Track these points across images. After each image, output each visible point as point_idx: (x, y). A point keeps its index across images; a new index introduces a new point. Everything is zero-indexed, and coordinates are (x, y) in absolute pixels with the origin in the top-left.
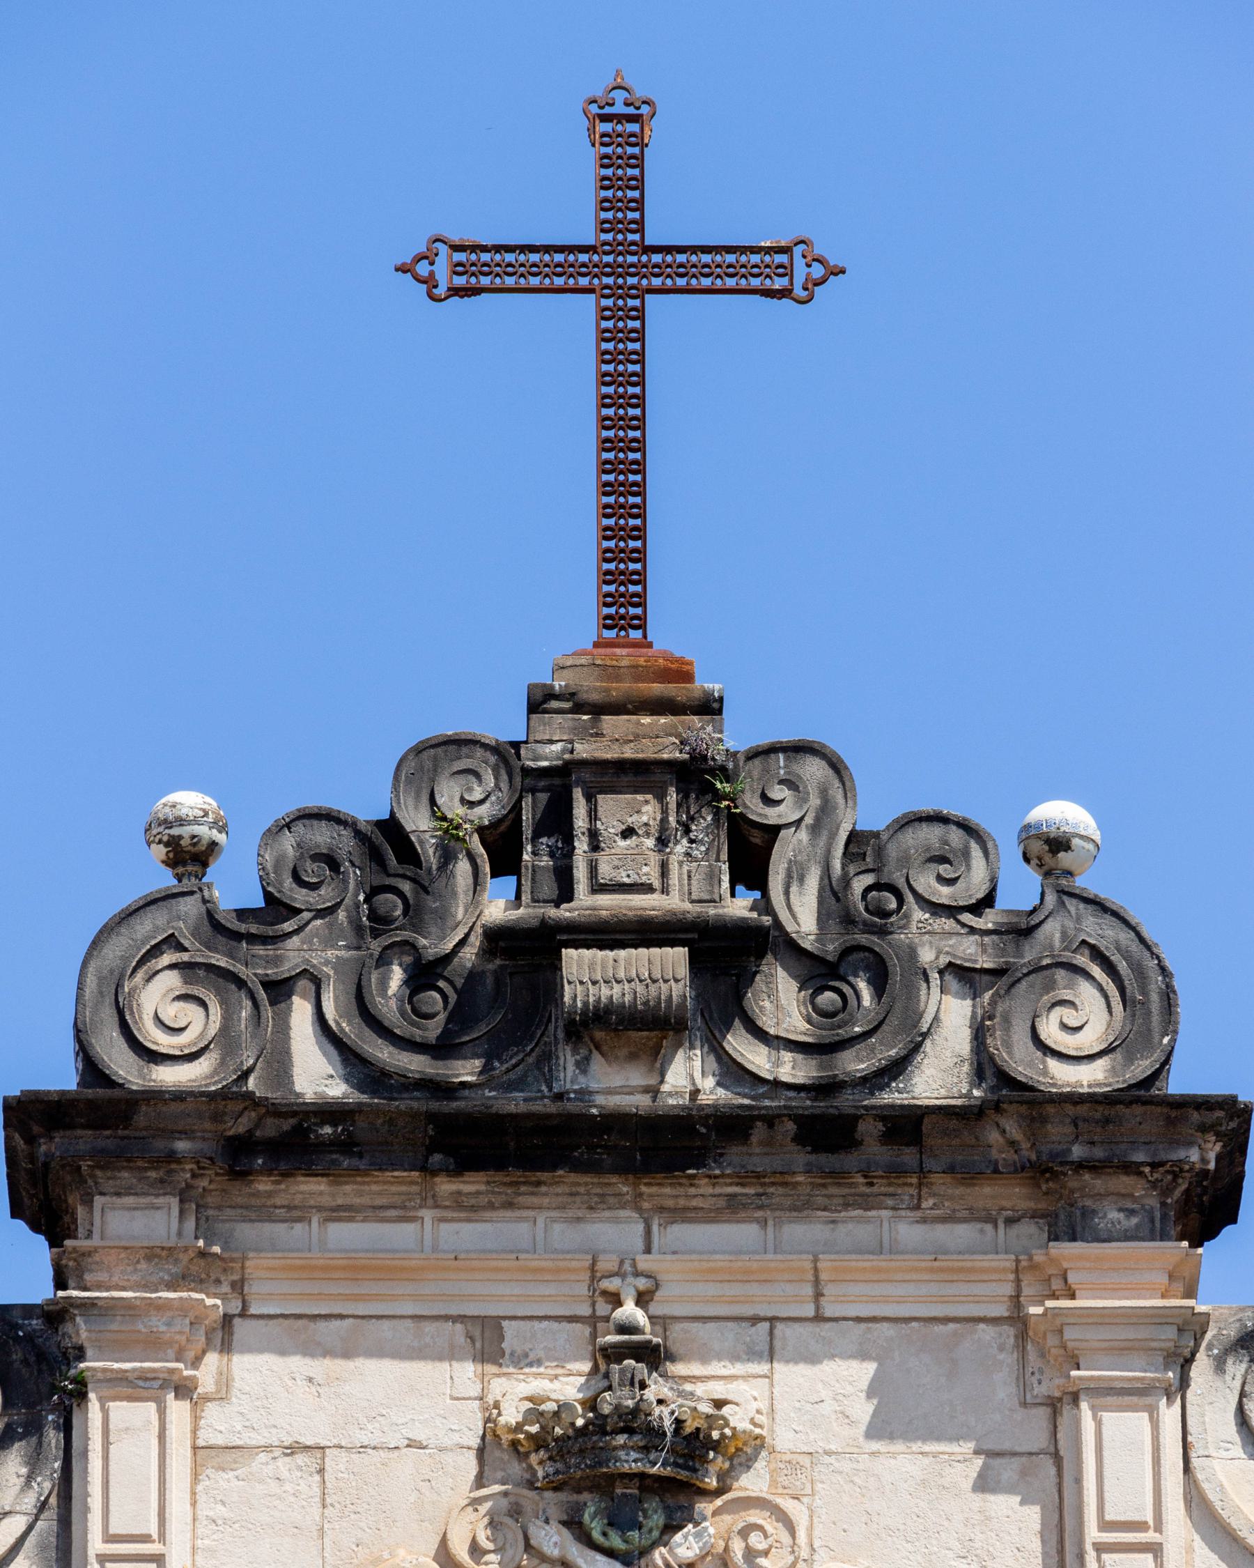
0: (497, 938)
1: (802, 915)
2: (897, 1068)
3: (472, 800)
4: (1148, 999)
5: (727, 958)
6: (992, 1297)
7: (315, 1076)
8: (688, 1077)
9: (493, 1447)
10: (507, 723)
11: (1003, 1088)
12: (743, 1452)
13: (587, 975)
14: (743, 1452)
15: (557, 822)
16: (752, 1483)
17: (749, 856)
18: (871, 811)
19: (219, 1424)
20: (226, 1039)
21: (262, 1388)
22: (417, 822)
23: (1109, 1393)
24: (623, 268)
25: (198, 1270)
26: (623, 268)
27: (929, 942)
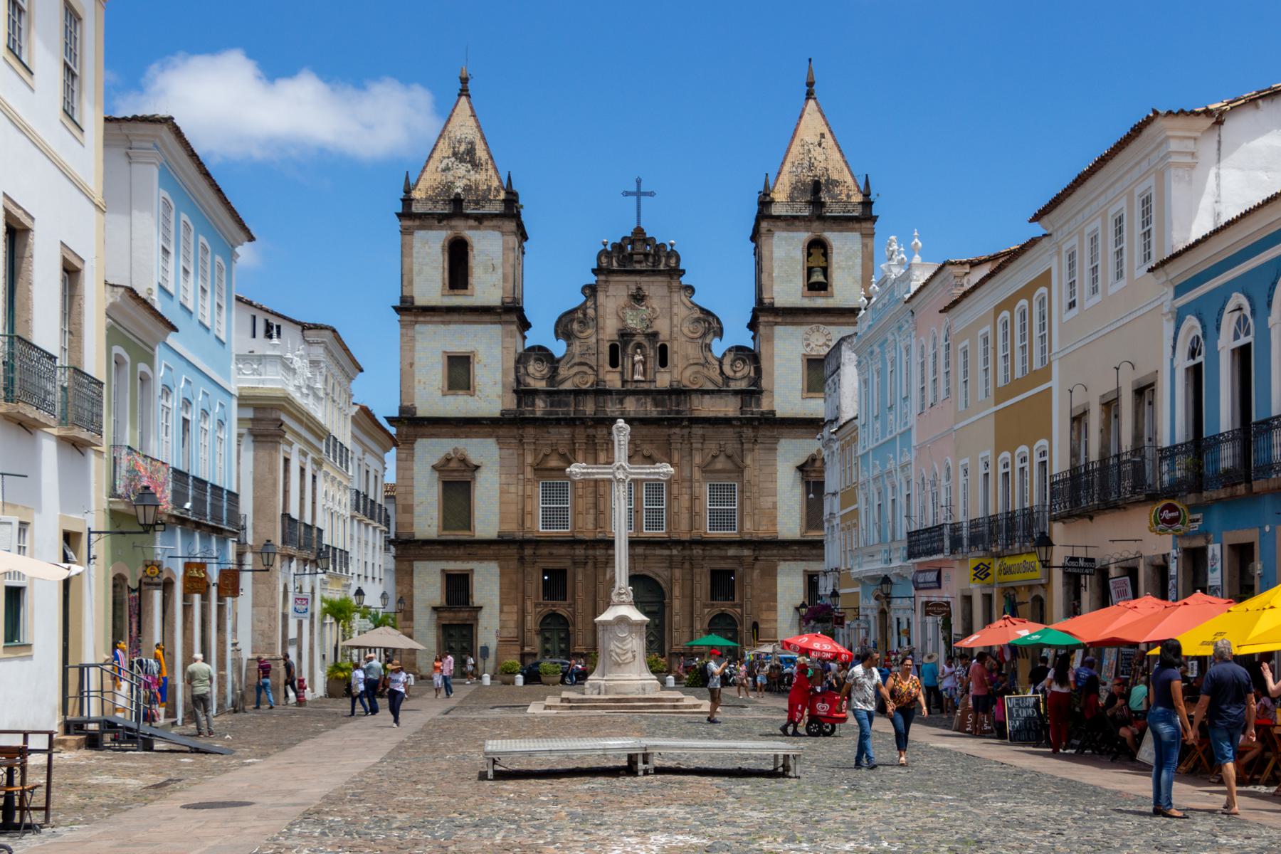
4: (678, 259)
5: (646, 255)
13: (636, 257)
26: (639, 194)
27: (661, 254)
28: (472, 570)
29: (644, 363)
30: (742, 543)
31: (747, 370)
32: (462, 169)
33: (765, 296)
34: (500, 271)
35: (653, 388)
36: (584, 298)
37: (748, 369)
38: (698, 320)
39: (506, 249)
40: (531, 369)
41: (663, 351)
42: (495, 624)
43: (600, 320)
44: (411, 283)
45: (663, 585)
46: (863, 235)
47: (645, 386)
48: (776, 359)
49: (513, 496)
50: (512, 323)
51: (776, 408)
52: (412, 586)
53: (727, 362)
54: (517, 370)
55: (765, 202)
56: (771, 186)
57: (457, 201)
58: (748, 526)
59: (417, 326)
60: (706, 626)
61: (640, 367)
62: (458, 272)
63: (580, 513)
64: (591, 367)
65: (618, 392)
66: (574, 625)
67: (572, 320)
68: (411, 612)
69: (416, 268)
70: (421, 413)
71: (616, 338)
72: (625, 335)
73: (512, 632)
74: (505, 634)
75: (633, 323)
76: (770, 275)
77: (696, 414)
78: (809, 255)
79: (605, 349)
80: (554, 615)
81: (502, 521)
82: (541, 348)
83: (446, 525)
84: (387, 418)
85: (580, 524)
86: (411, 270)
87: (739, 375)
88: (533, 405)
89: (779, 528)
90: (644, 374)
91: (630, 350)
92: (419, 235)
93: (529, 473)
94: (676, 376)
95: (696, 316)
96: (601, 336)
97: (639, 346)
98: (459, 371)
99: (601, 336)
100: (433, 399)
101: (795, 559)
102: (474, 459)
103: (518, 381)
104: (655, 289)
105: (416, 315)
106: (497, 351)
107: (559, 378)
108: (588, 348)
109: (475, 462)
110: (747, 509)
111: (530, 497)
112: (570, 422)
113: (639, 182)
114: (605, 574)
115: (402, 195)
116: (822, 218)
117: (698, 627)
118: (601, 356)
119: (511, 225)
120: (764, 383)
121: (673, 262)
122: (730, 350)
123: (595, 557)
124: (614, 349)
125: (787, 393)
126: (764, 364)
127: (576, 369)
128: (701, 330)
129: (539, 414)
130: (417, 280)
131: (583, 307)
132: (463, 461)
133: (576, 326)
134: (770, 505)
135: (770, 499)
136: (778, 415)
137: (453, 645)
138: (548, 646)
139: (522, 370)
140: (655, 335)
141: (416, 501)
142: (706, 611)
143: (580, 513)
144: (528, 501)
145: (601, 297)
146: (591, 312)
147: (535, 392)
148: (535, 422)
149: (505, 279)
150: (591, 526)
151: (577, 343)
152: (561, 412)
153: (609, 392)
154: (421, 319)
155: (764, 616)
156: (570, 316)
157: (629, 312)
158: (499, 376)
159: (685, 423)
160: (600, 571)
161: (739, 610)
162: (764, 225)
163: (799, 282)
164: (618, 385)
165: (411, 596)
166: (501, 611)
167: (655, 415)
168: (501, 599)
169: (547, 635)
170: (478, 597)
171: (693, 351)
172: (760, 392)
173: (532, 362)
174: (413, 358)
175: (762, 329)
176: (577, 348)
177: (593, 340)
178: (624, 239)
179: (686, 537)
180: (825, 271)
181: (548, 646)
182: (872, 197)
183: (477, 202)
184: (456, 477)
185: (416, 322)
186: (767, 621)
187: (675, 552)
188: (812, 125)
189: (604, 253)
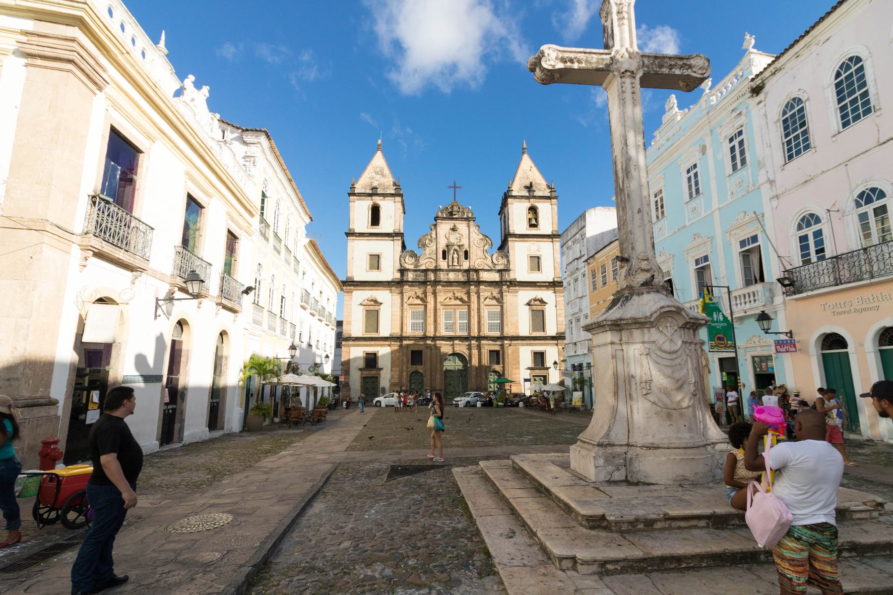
24: (455, 187)
26: (455, 187)
32: (378, 177)
37: (505, 261)
41: (466, 253)
42: (389, 376)
47: (458, 268)
53: (494, 257)
57: (375, 188)
61: (456, 260)
65: (446, 270)
70: (355, 279)
74: (393, 381)
75: (453, 240)
80: (416, 372)
82: (412, 251)
85: (428, 329)
91: (452, 252)
98: (375, 261)
100: (360, 273)
101: (527, 345)
102: (379, 300)
104: (462, 226)
112: (424, 283)
116: (535, 197)
120: (511, 267)
121: (470, 215)
124: (444, 252)
125: (520, 271)
126: (511, 258)
132: (376, 301)
146: (434, 236)
147: (408, 270)
153: (440, 270)
155: (514, 372)
162: (509, 200)
163: (525, 224)
164: (446, 268)
171: (480, 253)
175: (510, 243)
180: (536, 220)
184: (372, 308)
188: (526, 162)
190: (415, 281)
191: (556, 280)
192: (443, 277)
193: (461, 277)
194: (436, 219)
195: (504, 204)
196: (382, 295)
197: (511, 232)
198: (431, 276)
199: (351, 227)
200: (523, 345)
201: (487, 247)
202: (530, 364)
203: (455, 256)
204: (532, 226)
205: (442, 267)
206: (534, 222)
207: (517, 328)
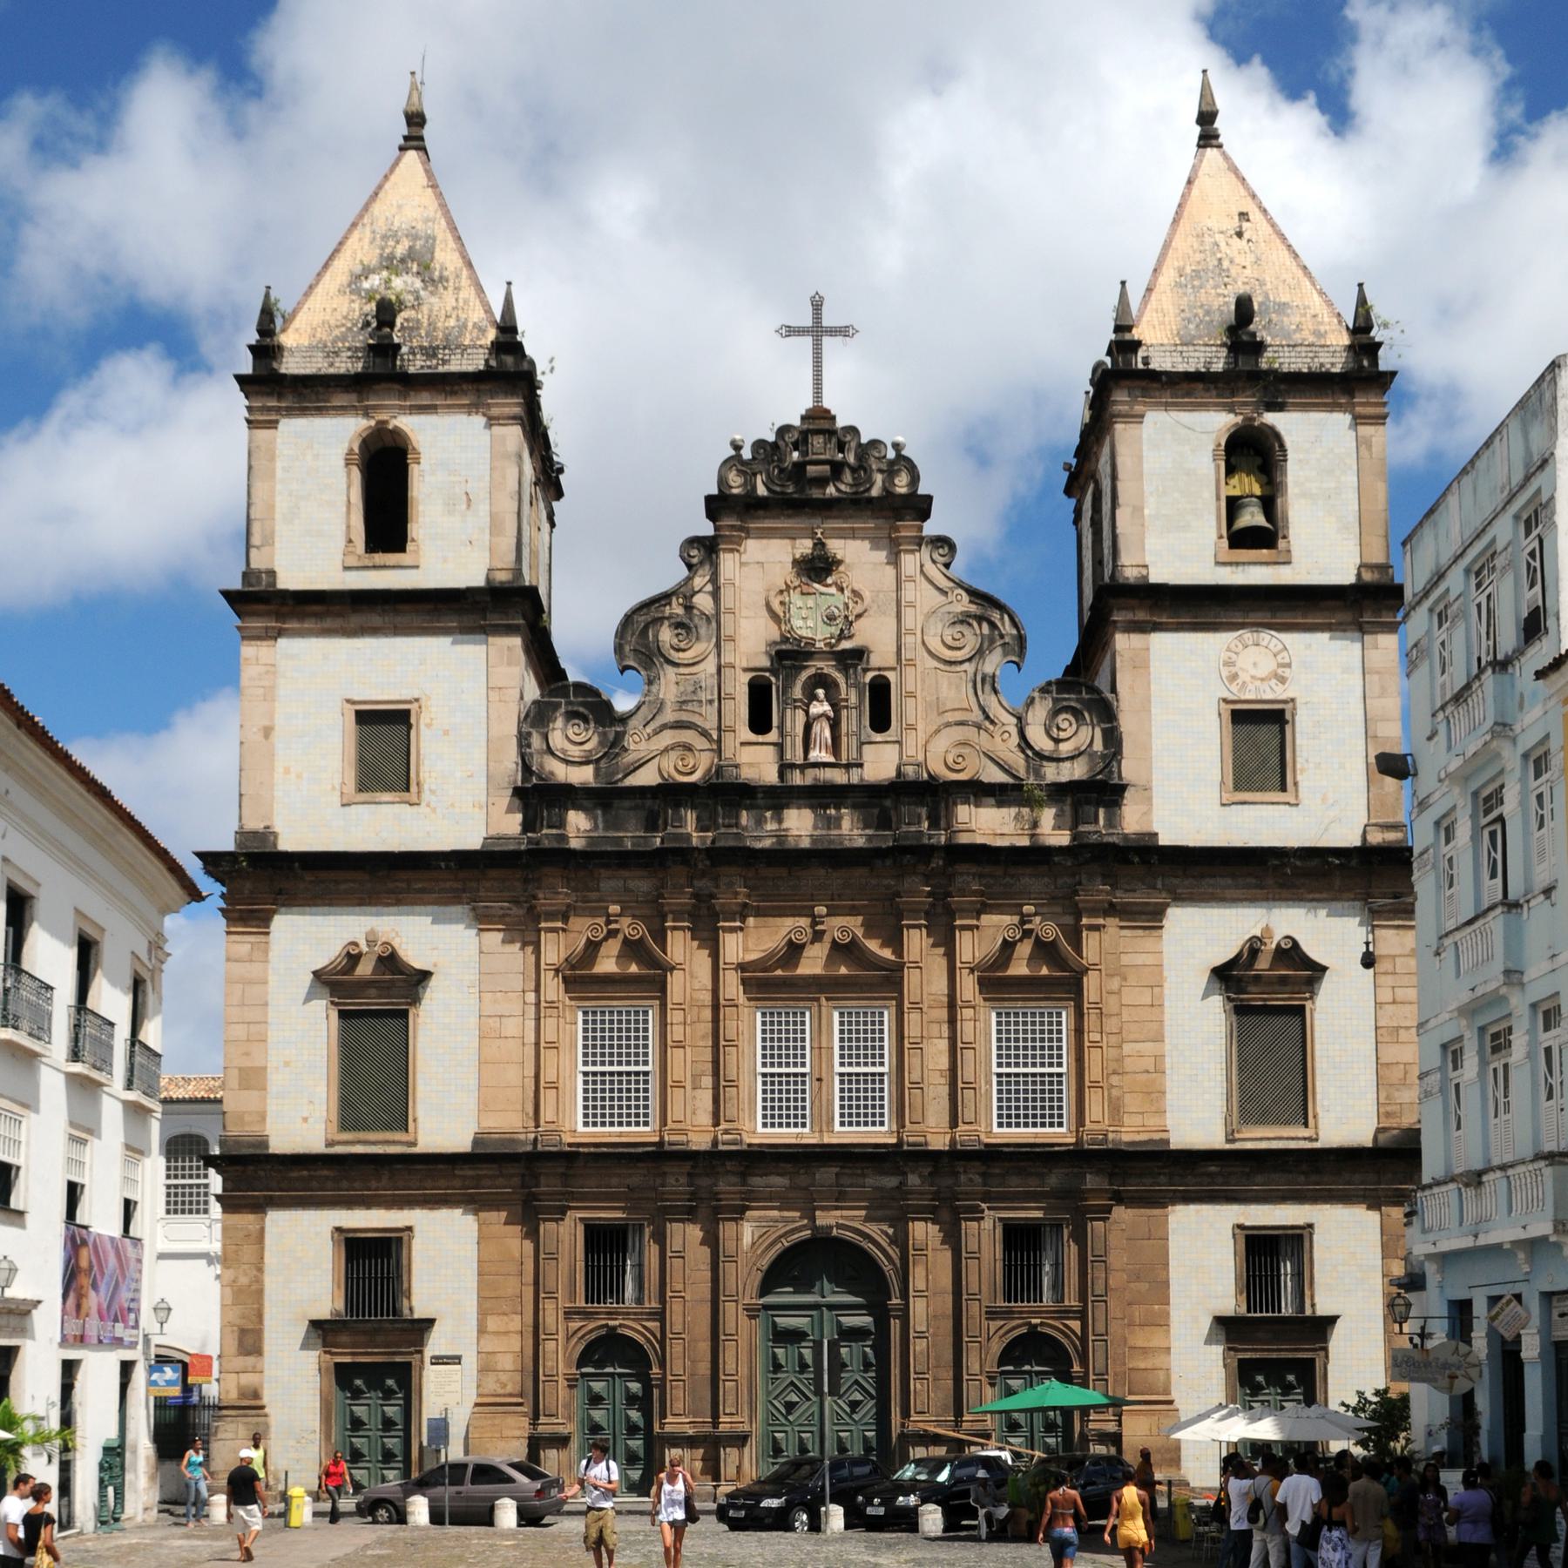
0: (795, 464)
1: (851, 459)
2: (868, 490)
3: (791, 437)
4: (915, 479)
5: (837, 468)
6: (885, 533)
7: (762, 491)
8: (831, 490)
9: (795, 562)
10: (797, 422)
11: (888, 493)
12: (840, 562)
14: (840, 562)
15: (805, 441)
16: (841, 568)
17: (841, 447)
18: (864, 440)
19: (744, 558)
20: (744, 485)
21: (753, 548)
22: (781, 443)
23: (907, 551)
24: (818, 331)
25: (741, 529)
26: (818, 331)
28: (410, 1229)
29: (835, 725)
30: (1079, 1157)
31: (1083, 736)
33: (1125, 559)
34: (483, 509)
35: (855, 780)
36: (685, 572)
38: (964, 620)
39: (496, 455)
40: (557, 739)
43: (726, 619)
44: (269, 540)
45: (887, 1267)
46: (1358, 420)
47: (838, 777)
48: (1155, 710)
49: (513, 1045)
50: (509, 630)
51: (1156, 828)
52: (260, 1270)
54: (523, 740)
55: (1124, 345)
56: (1134, 312)
58: (1096, 1109)
59: (282, 642)
60: (991, 1366)
61: (823, 731)
62: (386, 517)
63: (679, 1085)
64: (705, 734)
65: (770, 791)
66: (662, 1365)
67: (659, 621)
68: (258, 1333)
69: (282, 504)
70: (287, 844)
71: (766, 663)
72: (789, 655)
73: (508, 1379)
74: (491, 1385)
76: (1138, 510)
77: (964, 839)
78: (1230, 471)
79: (739, 688)
81: (483, 1107)
83: (350, 1115)
84: (201, 855)
85: (675, 1112)
86: (271, 508)
87: (1065, 748)
88: (562, 824)
89: (1170, 1122)
90: (835, 747)
92: (291, 427)
93: (553, 988)
94: (912, 750)
95: (959, 608)
96: (727, 658)
97: (821, 680)
99: (727, 658)
102: (415, 957)
103: (527, 769)
105: (280, 617)
106: (474, 693)
107: (629, 758)
108: (698, 687)
109: (417, 965)
110: (1094, 1071)
111: (553, 1046)
113: (817, 305)
114: (738, 1239)
115: (253, 337)
117: (975, 1368)
118: (728, 706)
119: (512, 405)
120: (1129, 769)
121: (901, 485)
122: (1044, 690)
123: (715, 1196)
125: (1181, 793)
127: (668, 738)
128: (971, 642)
129: (575, 844)
130: (281, 529)
131: (683, 592)
132: (390, 961)
133: (666, 635)
134: (1148, 1063)
135: (1148, 1048)
136: (1164, 840)
137: (360, 1411)
138: (598, 1415)
139: (536, 742)
140: (859, 654)
141: (274, 1059)
142: (994, 1325)
143: (679, 1085)
144: (548, 1057)
145: (728, 562)
146: (703, 602)
147: (568, 795)
148: (562, 858)
149: (495, 526)
150: (705, 1119)
151: (670, 670)
152: (630, 836)
154: (292, 625)
155: (1139, 1339)
156: (654, 614)
157: (795, 597)
158: (479, 755)
159: (937, 862)
160: (727, 1230)
161: (1076, 1325)
162: (1120, 398)
163: (1208, 529)
165: (260, 1293)
166: (482, 1331)
167: (860, 842)
168: (481, 1299)
169: (598, 1386)
170: (422, 1298)
171: (954, 690)
172: (1122, 788)
173: (559, 723)
174: (272, 718)
175: (1123, 642)
176: (669, 685)
177: (710, 666)
178: (783, 431)
179: (939, 1143)
180: (1269, 504)
181: (598, 1415)
182: (1377, 334)
183: (431, 352)
185: (280, 633)
186: (1145, 1351)
187: (913, 1180)
189: (735, 461)
190: (606, 861)
191: (1376, 838)
192: (760, 831)
193: (851, 830)
194: (716, 506)
195: (1096, 430)
196: (423, 936)
197: (1130, 574)
198: (690, 826)
199: (257, 562)
200: (1187, 1199)
201: (993, 662)
202: (1229, 1302)
203: (820, 708)
204: (1243, 539)
205: (747, 774)
206: (1252, 517)
207: (1154, 1095)
